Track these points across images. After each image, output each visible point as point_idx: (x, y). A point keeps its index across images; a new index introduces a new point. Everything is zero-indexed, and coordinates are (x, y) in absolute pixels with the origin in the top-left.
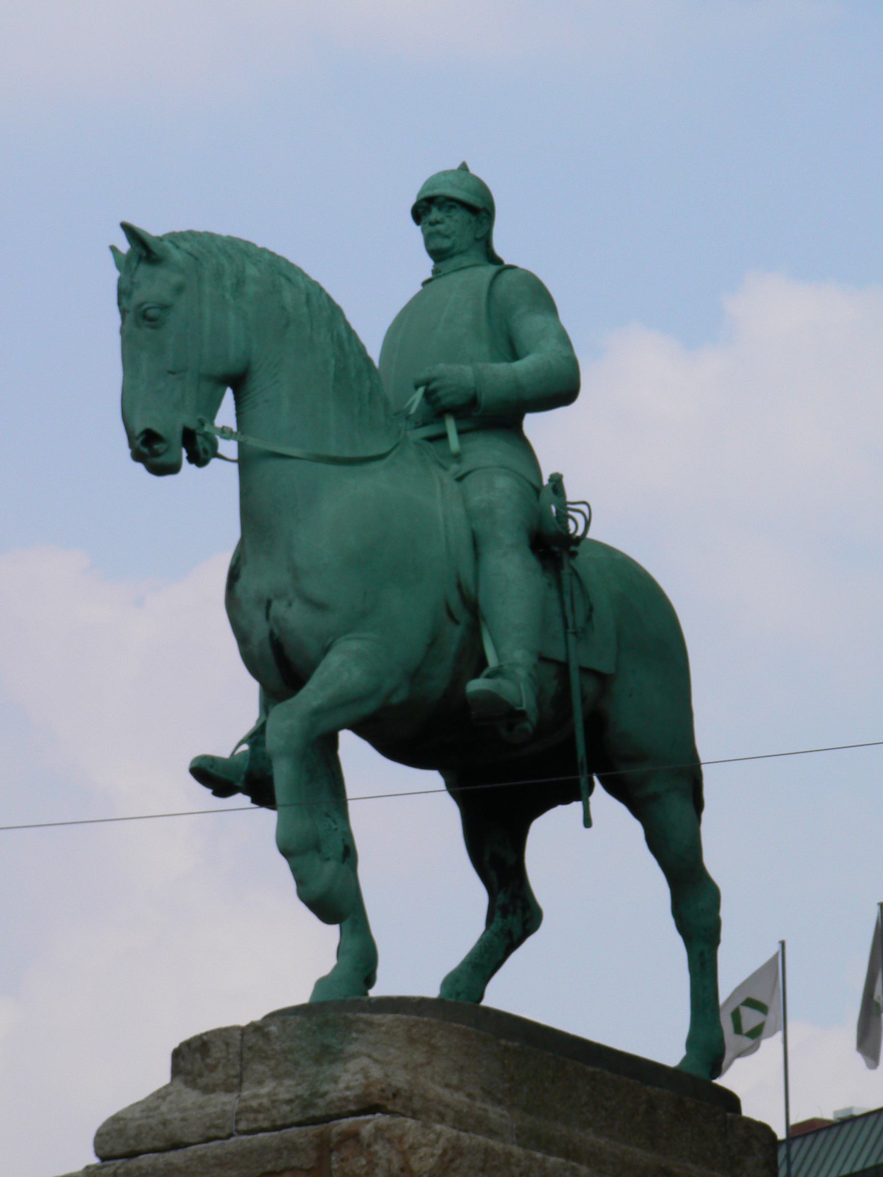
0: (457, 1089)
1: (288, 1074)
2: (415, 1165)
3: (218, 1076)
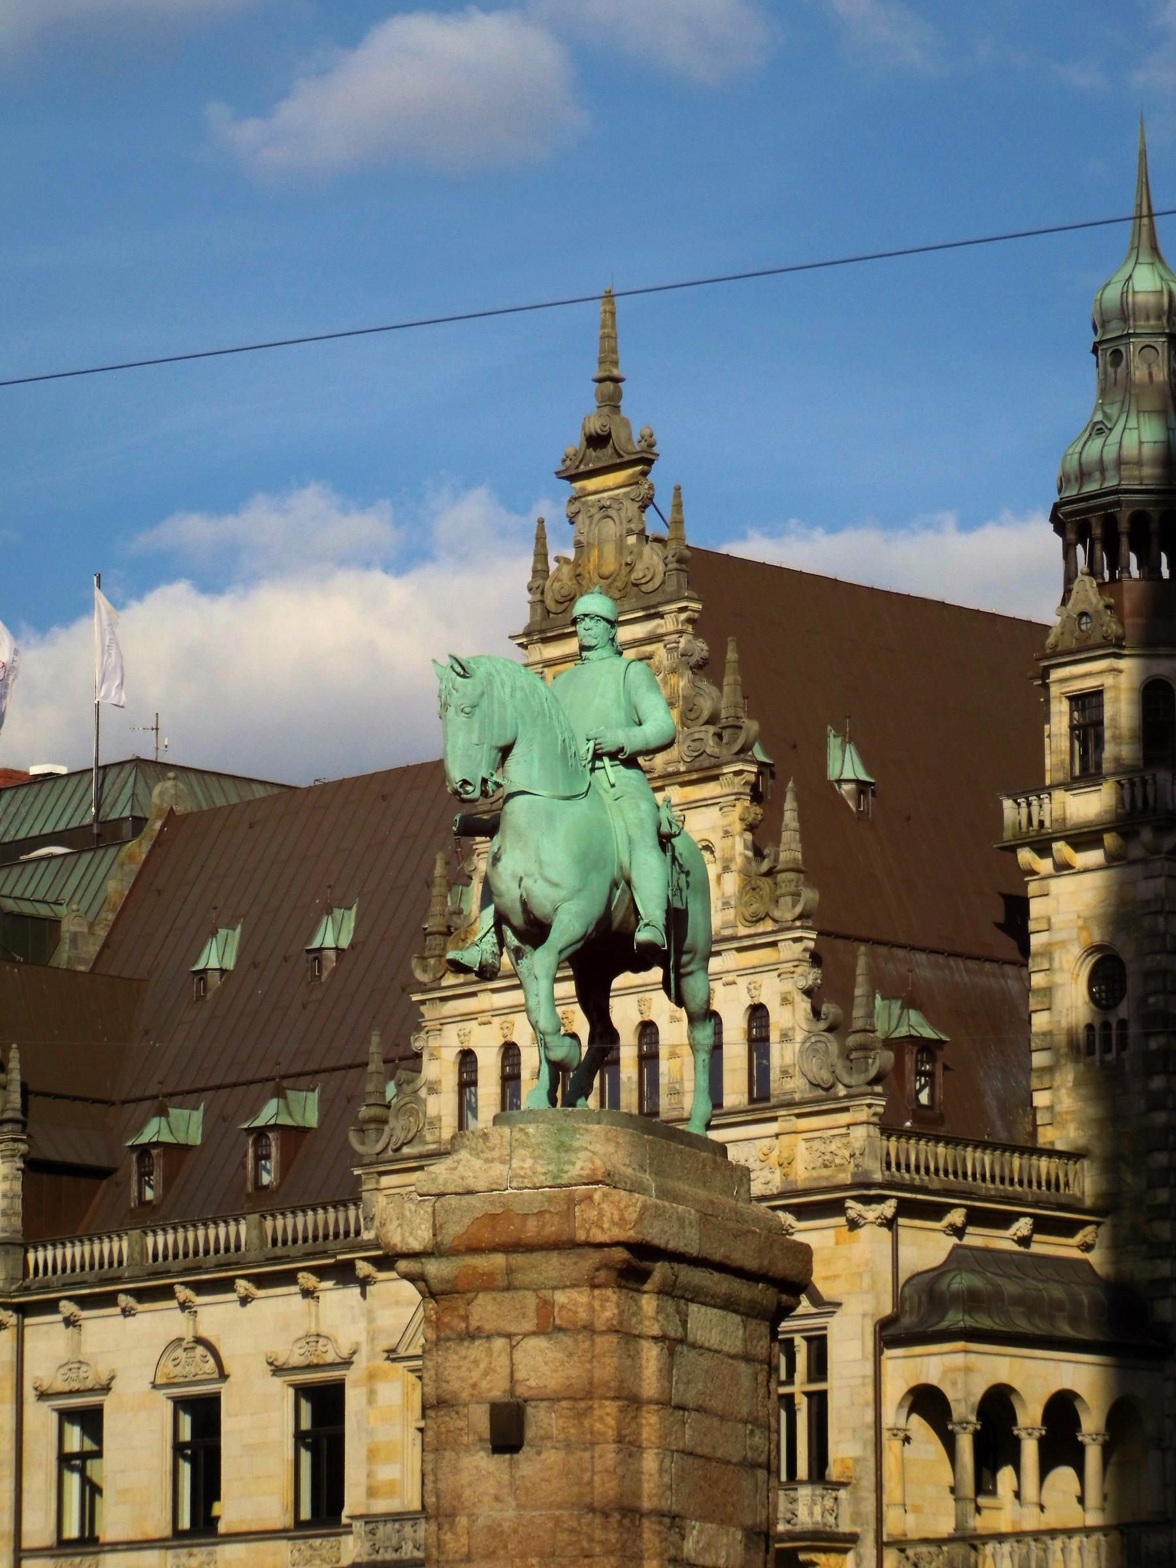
0: (629, 1166)
1: (540, 1157)
2: (626, 1215)
3: (496, 1154)
